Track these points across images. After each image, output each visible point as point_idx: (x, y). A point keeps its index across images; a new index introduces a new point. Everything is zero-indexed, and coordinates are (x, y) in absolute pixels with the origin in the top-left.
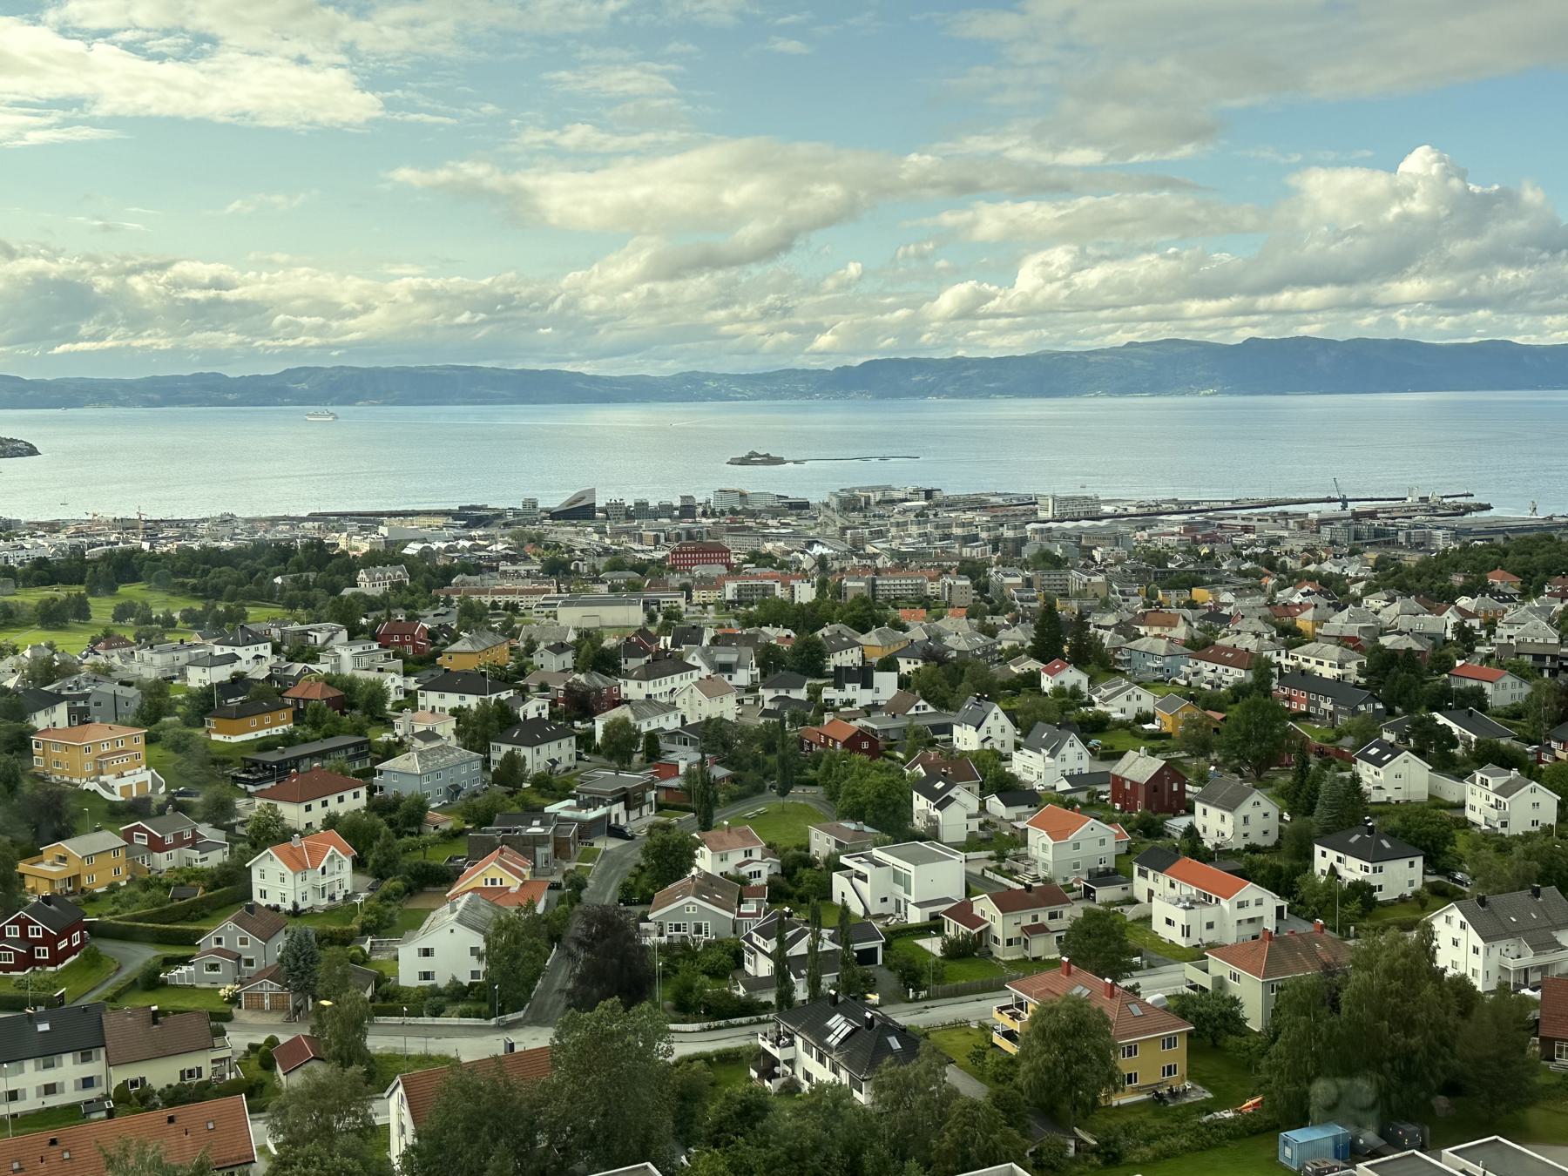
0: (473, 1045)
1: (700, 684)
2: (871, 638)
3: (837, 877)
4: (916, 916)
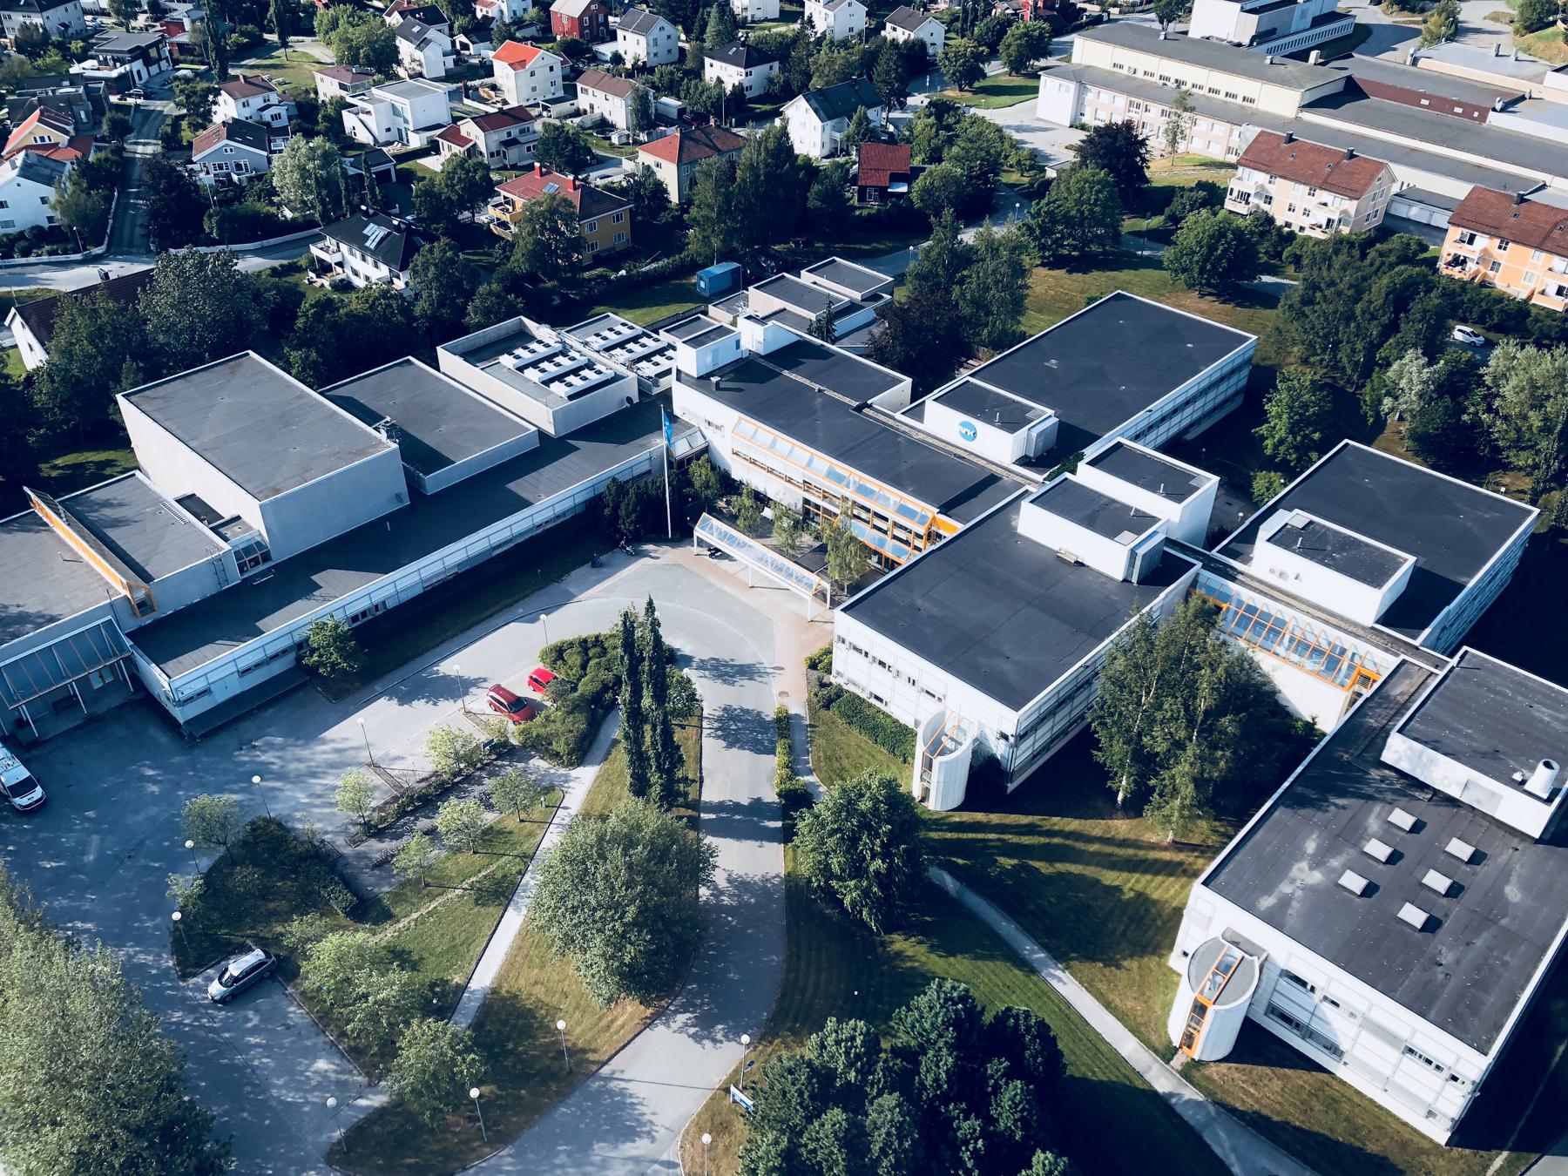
3: (344, 113)
4: (416, 142)
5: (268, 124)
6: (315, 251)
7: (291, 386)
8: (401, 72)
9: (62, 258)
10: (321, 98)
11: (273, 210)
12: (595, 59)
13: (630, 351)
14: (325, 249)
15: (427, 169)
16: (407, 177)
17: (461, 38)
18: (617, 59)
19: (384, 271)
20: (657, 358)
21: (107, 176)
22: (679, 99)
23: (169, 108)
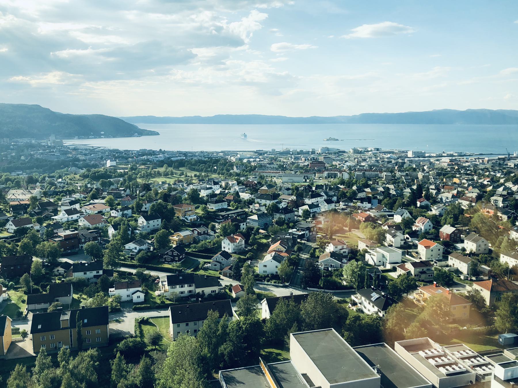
0: (280, 292)
1: (325, 200)
2: (368, 190)
3: (366, 254)
4: (389, 267)
5: (342, 254)
6: (353, 297)
7: (344, 344)
8: (386, 244)
9: (277, 284)
10: (359, 248)
11: (340, 281)
12: (456, 249)
13: (472, 362)
14: (357, 298)
15: (390, 276)
16: (385, 278)
17: (408, 236)
18: (464, 250)
19: (376, 309)
20: (484, 367)
21: (295, 263)
22: (489, 267)
23: (314, 245)
